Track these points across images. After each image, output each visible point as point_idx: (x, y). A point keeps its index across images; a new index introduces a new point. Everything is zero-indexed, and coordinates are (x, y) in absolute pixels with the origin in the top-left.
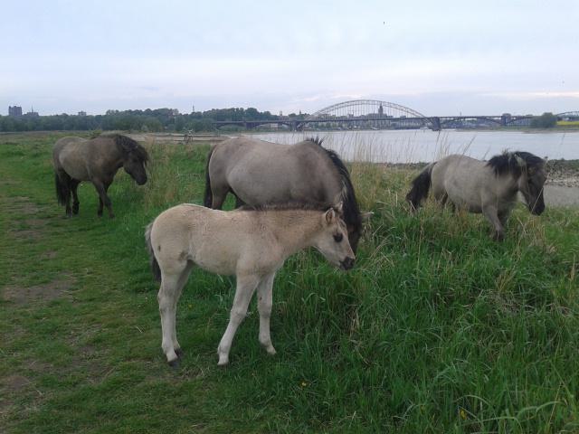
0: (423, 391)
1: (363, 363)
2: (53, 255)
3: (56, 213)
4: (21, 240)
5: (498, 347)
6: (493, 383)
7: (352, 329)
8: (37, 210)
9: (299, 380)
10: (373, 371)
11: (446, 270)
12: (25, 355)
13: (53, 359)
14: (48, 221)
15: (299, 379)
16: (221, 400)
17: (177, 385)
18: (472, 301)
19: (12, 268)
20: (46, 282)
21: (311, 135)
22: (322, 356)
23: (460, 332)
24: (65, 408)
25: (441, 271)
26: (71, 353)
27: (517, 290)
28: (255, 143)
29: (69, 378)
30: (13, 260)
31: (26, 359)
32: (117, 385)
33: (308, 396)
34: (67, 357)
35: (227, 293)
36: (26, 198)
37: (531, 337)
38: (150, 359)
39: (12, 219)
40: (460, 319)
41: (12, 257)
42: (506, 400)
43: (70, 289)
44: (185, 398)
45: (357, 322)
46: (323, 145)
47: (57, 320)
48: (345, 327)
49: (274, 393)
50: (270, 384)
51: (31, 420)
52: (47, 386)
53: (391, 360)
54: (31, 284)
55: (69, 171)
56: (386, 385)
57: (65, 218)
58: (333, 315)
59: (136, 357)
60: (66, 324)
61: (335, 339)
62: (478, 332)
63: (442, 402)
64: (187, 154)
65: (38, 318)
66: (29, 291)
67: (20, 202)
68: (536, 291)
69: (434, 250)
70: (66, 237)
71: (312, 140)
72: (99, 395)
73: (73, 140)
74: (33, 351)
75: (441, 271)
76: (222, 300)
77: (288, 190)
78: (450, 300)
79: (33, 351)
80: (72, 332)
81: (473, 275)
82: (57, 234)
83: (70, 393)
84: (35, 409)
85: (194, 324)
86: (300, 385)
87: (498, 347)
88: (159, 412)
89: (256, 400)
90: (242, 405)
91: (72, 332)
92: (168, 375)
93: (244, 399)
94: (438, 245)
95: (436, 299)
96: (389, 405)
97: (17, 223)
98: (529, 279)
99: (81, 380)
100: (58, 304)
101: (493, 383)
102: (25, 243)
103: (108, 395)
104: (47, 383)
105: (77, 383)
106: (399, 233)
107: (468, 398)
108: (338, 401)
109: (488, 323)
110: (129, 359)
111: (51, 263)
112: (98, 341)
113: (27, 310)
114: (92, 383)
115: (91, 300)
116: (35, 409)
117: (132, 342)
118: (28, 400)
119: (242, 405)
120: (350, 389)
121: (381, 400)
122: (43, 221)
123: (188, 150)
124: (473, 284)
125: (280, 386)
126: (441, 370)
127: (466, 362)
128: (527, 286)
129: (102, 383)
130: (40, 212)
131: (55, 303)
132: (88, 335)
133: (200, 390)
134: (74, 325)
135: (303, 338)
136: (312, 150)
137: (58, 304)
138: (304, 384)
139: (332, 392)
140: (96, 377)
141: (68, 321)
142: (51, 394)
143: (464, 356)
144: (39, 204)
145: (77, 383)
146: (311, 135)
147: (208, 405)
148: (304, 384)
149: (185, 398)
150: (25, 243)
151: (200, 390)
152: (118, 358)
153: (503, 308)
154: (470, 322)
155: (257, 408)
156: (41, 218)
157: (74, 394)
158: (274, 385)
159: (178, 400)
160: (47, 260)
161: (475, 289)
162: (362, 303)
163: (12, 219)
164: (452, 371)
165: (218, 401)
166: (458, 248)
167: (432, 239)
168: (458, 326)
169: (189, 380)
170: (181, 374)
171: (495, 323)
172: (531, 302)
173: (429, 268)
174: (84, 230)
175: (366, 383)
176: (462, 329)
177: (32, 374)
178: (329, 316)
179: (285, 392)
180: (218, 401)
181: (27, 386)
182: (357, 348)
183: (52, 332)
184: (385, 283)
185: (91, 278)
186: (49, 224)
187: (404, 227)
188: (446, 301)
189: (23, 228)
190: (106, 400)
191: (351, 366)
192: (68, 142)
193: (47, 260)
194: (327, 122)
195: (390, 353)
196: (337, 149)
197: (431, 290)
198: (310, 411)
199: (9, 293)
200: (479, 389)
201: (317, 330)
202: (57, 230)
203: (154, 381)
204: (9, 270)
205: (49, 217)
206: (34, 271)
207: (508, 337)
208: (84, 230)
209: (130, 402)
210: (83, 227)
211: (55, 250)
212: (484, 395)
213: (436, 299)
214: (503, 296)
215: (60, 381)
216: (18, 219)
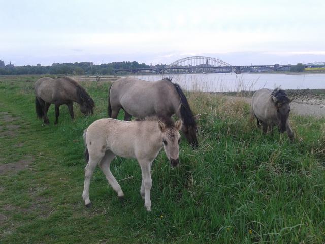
0: (228, 219)
1: (195, 204)
2: (21, 145)
4: (3, 137)
5: (270, 194)
6: (268, 214)
7: (190, 185)
8: (12, 120)
9: (159, 214)
10: (200, 208)
11: (242, 151)
12: (5, 202)
13: (20, 204)
14: (19, 126)
15: (159, 214)
16: (115, 226)
17: (91, 218)
18: (257, 168)
22: (172, 201)
23: (249, 186)
24: (26, 232)
25: (239, 151)
26: (31, 201)
27: (281, 162)
28: (135, 81)
29: (29, 215)
31: (6, 204)
32: (56, 218)
33: (165, 223)
34: (28, 203)
35: (120, 166)
37: (289, 188)
38: (75, 203)
40: (250, 179)
42: (274, 224)
43: (31, 165)
44: (95, 225)
45: (192, 181)
47: (23, 182)
48: (185, 184)
49: (145, 222)
50: (143, 217)
51: (6, 239)
52: (16, 220)
53: (211, 202)
54: (9, 162)
56: (208, 216)
58: (178, 177)
59: (67, 203)
60: (28, 184)
61: (180, 191)
62: (260, 186)
63: (239, 226)
65: (11, 181)
66: (7, 166)
67: (3, 115)
68: (292, 162)
69: (236, 140)
70: (28, 135)
71: (167, 79)
72: (46, 224)
74: (9, 200)
75: (239, 151)
76: (116, 169)
77: (153, 107)
78: (244, 168)
79: (9, 200)
80: (32, 189)
81: (257, 154)
82: (24, 133)
83: (29, 223)
84: (9, 233)
85: (101, 183)
86: (160, 217)
87: (270, 194)
88: (80, 233)
89: (135, 226)
90: (127, 229)
91: (32, 189)
92: (86, 212)
93: (129, 225)
94: (238, 137)
95: (236, 168)
96: (209, 227)
98: (288, 156)
99: (36, 216)
100: (24, 172)
101: (268, 214)
102: (6, 138)
103: (52, 224)
104: (16, 218)
105: (34, 218)
106: (216, 130)
107: (254, 223)
108: (181, 225)
109: (266, 179)
110: (64, 203)
111: (20, 150)
112: (46, 193)
113: (6, 177)
114: (43, 217)
115: (42, 170)
116: (9, 233)
117: (65, 194)
118: (5, 228)
119: (127, 229)
120: (188, 219)
121: (205, 225)
122: (15, 126)
123: (99, 85)
124: (257, 159)
125: (149, 218)
126: (239, 207)
127: (252, 202)
128: (287, 160)
129: (48, 217)
132: (40, 190)
133: (103, 221)
134: (33, 185)
135: (162, 190)
136: (166, 84)
137: (24, 172)
138: (162, 216)
139: (178, 221)
140: (44, 214)
141: (29, 182)
142: (18, 225)
143: (252, 199)
145: (34, 218)
147: (107, 229)
148: (162, 216)
149: (95, 225)
150: (6, 138)
151: (103, 221)
152: (57, 203)
153: (274, 172)
154: (255, 180)
155: (135, 230)
156: (16, 124)
157: (32, 224)
158: (145, 217)
159: (91, 226)
160: (18, 148)
161: (258, 161)
162: (195, 170)
164: (244, 208)
165: (114, 226)
166: (249, 139)
167: (234, 134)
168: (249, 182)
169: (98, 215)
170: (93, 212)
171: (269, 181)
172: (289, 169)
173: (233, 151)
174: (39, 131)
175: (197, 215)
176: (251, 184)
177: (8, 213)
178: (176, 178)
179: (151, 221)
180: (114, 226)
181: (5, 220)
182: (192, 196)
183: (20, 189)
184: (208, 159)
185: (42, 158)
186: (20, 128)
187: (219, 127)
188: (242, 169)
189: (4, 130)
190: (50, 227)
191: (188, 206)
193: (18, 148)
194: (177, 69)
195: (210, 199)
197: (234, 163)
198: (165, 231)
200: (259, 218)
201: (170, 186)
202: (24, 131)
203: (77, 216)
206: (10, 154)
207: (276, 188)
208: (39, 131)
209: (64, 228)
210: (38, 129)
211: (23, 142)
212: (262, 221)
213: (236, 168)
214: (274, 166)
215: (24, 216)
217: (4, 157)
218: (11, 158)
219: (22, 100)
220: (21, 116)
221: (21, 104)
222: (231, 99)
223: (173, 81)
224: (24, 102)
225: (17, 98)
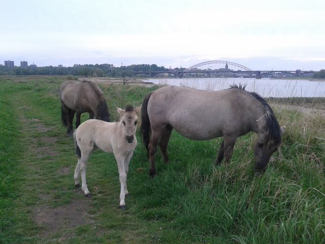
3: (59, 132)
4: (40, 156)
8: (46, 129)
14: (56, 139)
19: (38, 185)
20: (68, 203)
21: (238, 81)
30: (37, 177)
36: (36, 120)
39: (31, 137)
41: (37, 173)
46: (246, 89)
55: (67, 104)
57: (67, 137)
64: (130, 92)
66: (56, 214)
67: (34, 123)
73: (71, 83)
97: (34, 140)
100: (85, 231)
102: (44, 159)
115: (112, 227)
123: (130, 89)
130: (48, 131)
131: (82, 231)
137: (85, 231)
144: (46, 125)
146: (238, 81)
150: (44, 159)
156: (51, 136)
160: (63, 177)
163: (31, 137)
186: (57, 142)
189: (40, 145)
192: (69, 83)
196: (256, 92)
199: (42, 216)
204: (36, 187)
205: (56, 136)
206: (55, 188)
211: (67, 166)
216: (35, 137)
217: (48, 193)
218: (58, 197)
219: (52, 104)
220: (55, 125)
221: (51, 109)
222: (307, 112)
223: (249, 89)
224: (54, 106)
225: (47, 101)
